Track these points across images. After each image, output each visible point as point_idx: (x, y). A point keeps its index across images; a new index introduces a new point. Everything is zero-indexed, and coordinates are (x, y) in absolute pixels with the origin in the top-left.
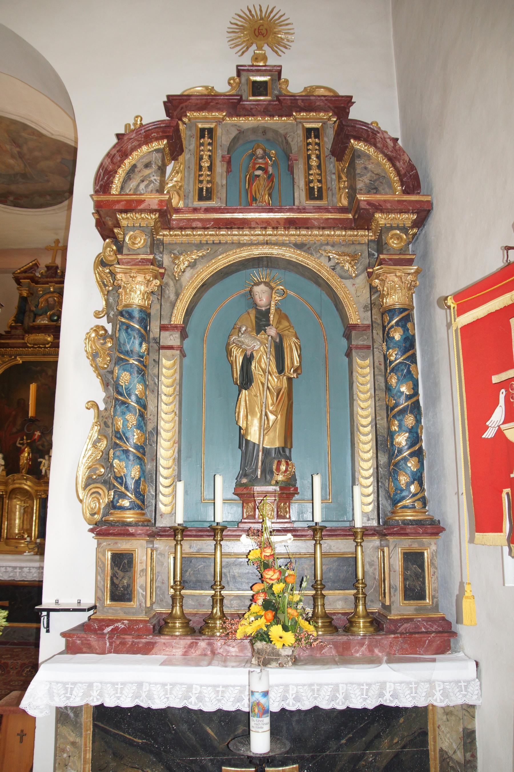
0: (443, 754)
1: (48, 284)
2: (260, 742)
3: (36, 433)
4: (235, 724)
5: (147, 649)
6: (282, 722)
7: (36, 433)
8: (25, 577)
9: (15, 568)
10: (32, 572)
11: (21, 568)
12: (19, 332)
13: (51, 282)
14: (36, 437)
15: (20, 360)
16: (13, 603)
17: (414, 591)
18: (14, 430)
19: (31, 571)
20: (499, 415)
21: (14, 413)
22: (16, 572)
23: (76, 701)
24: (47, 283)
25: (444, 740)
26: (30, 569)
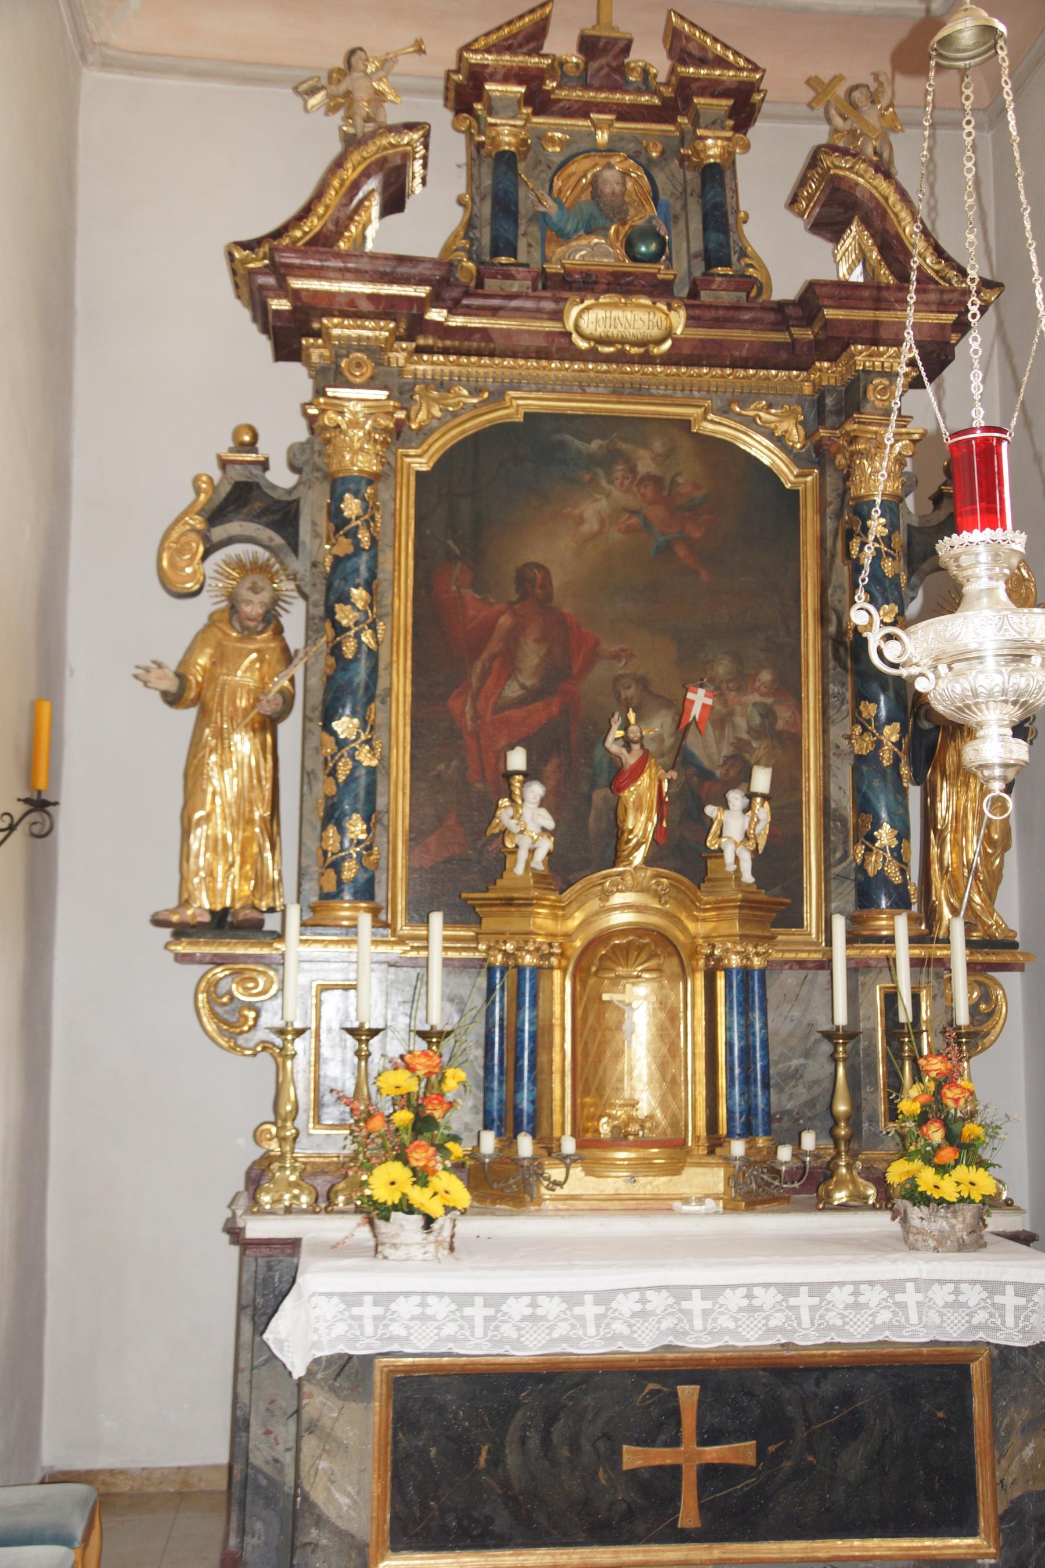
1: (586, 116)
3: (690, 696)
7: (690, 696)
8: (839, 1330)
9: (789, 1289)
10: (866, 1306)
11: (819, 1289)
13: (603, 108)
14: (696, 711)
15: (521, 404)
16: (771, 1449)
18: (512, 690)
19: (862, 1300)
21: (505, 621)
22: (795, 1309)
24: (583, 110)
26: (856, 1293)
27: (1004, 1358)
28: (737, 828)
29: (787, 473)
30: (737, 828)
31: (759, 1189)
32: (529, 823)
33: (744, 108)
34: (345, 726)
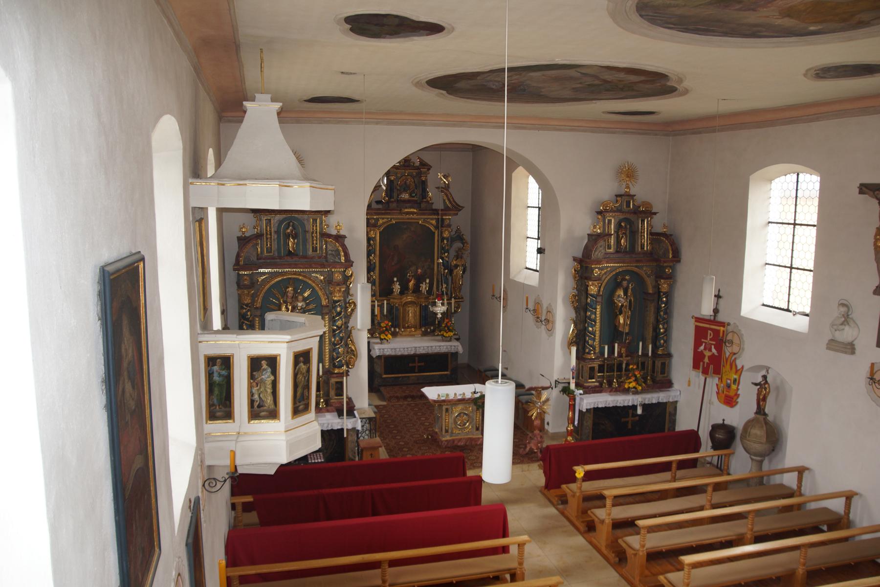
0: (670, 413)
2: (639, 411)
4: (634, 407)
5: (600, 392)
6: (645, 406)
12: (394, 205)
17: (663, 372)
20: (702, 348)
23: (592, 407)
25: (669, 409)
27: (452, 353)
28: (424, 287)
29: (432, 228)
30: (424, 287)
31: (425, 334)
32: (397, 287)
33: (429, 169)
34: (372, 273)
